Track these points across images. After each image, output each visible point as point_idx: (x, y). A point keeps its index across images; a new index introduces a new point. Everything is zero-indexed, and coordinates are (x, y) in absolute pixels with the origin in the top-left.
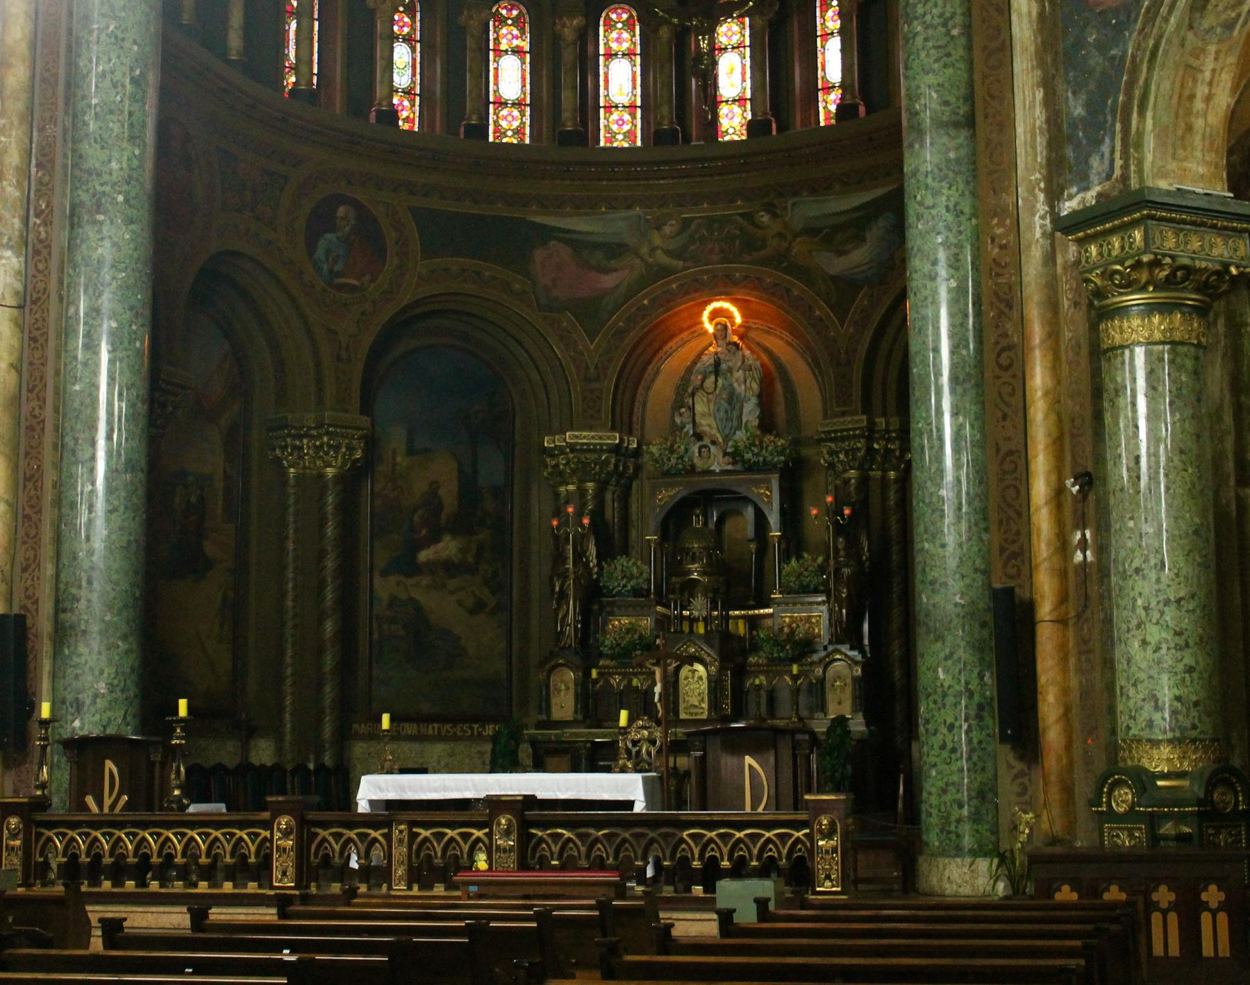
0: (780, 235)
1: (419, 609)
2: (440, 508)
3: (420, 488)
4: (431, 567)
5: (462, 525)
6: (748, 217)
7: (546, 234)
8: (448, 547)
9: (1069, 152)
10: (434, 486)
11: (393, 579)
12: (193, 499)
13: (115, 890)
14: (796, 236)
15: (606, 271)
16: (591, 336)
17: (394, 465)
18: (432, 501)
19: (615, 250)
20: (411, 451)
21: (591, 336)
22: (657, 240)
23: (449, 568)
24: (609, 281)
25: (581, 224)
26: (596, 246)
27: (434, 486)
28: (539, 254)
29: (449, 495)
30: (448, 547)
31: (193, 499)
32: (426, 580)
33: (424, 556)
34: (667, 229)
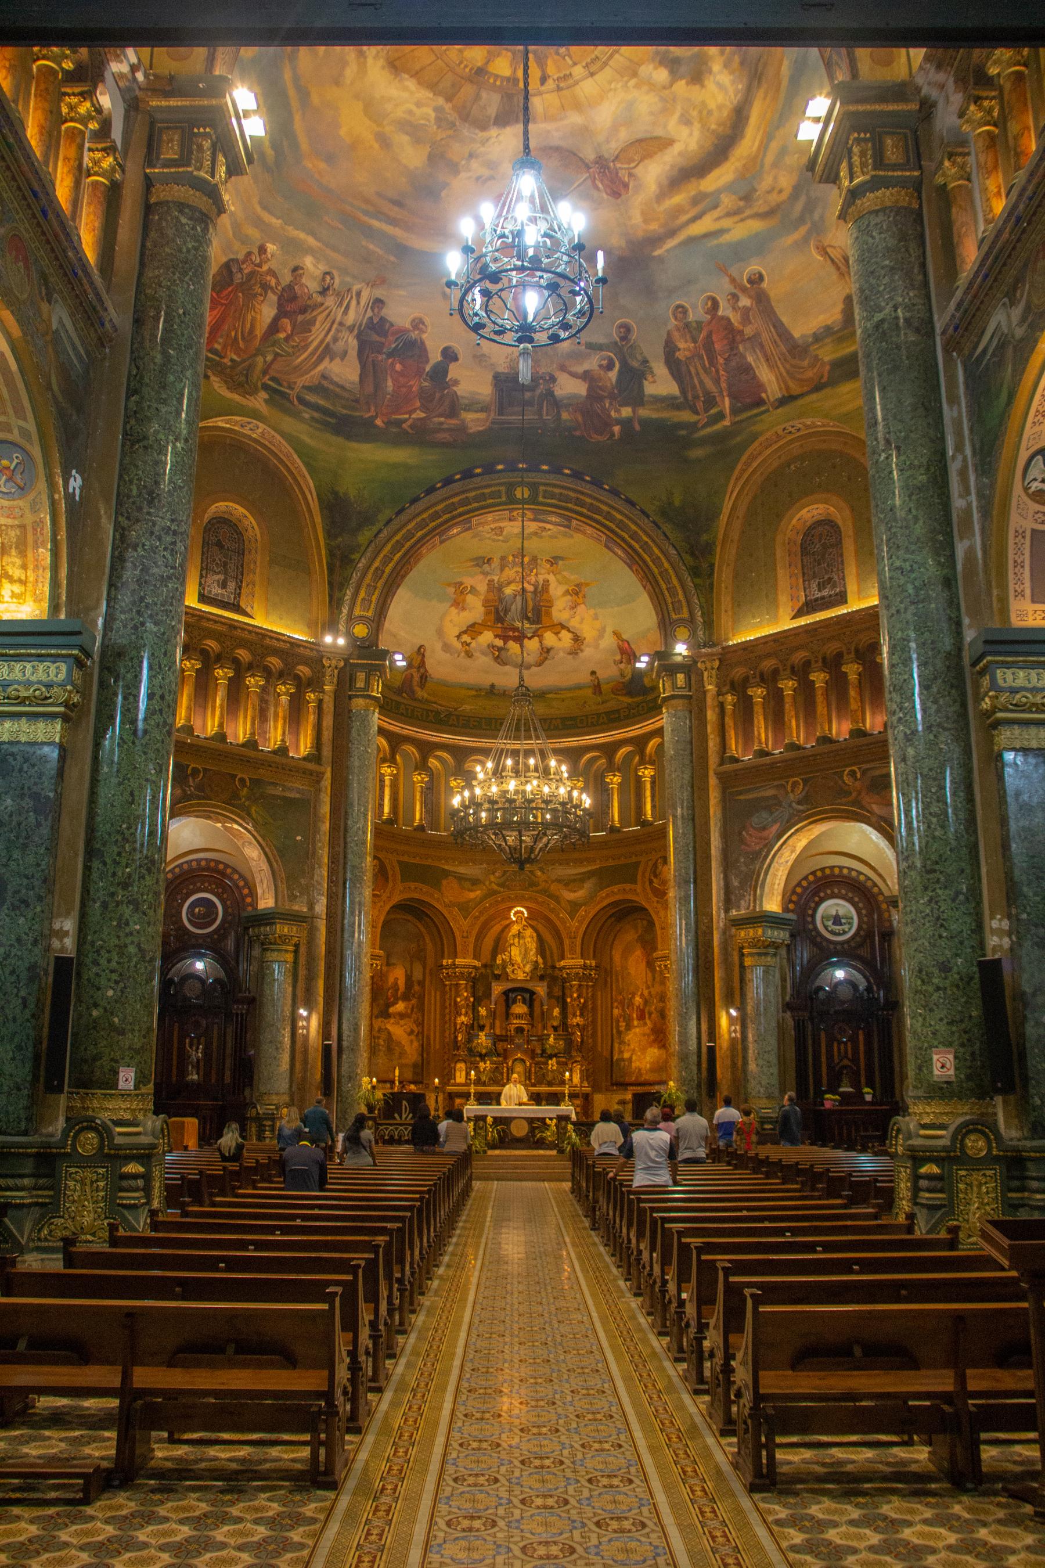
1: (389, 1033)
3: (391, 980)
4: (394, 1015)
5: (406, 998)
7: (446, 874)
8: (400, 1006)
9: (733, 898)
10: (397, 979)
16: (465, 918)
19: (475, 882)
21: (465, 918)
22: (492, 879)
23: (402, 1016)
25: (462, 870)
26: (466, 879)
28: (444, 882)
29: (402, 983)
33: (391, 1010)
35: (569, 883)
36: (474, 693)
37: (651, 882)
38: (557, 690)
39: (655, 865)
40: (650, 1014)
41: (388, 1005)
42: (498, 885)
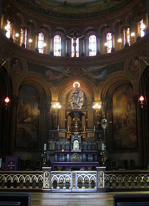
0: (86, 72)
3: (25, 109)
4: (26, 123)
6: (81, 69)
11: (20, 124)
13: (8, 189)
14: (89, 72)
15: (58, 76)
17: (21, 105)
19: (59, 73)
20: (24, 103)
24: (58, 77)
26: (55, 72)
32: (25, 125)
33: (25, 121)
34: (67, 70)
35: (95, 73)
36: (58, 4)
37: (130, 68)
38: (89, 3)
39: (131, 61)
40: (129, 121)
42: (67, 74)
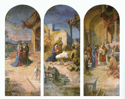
1: (57, 70)
2: (62, 44)
3: (56, 39)
4: (59, 60)
5: (68, 49)
8: (64, 54)
10: (60, 39)
11: (49, 62)
12: (24, 47)
17: (49, 33)
18: (59, 44)
20: (54, 30)
23: (65, 60)
27: (60, 39)
30: (64, 54)
31: (24, 47)
32: (58, 63)
33: (58, 56)
41: (55, 54)
